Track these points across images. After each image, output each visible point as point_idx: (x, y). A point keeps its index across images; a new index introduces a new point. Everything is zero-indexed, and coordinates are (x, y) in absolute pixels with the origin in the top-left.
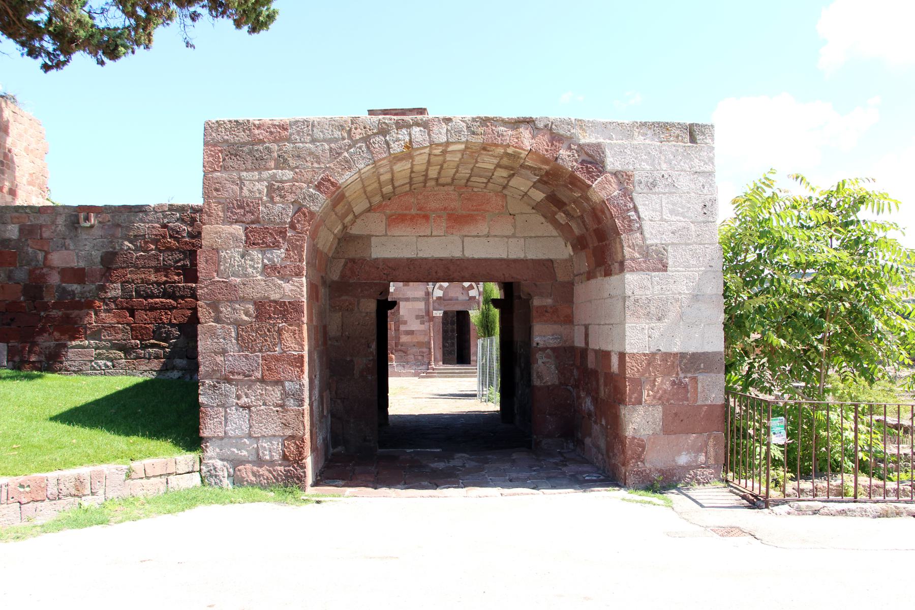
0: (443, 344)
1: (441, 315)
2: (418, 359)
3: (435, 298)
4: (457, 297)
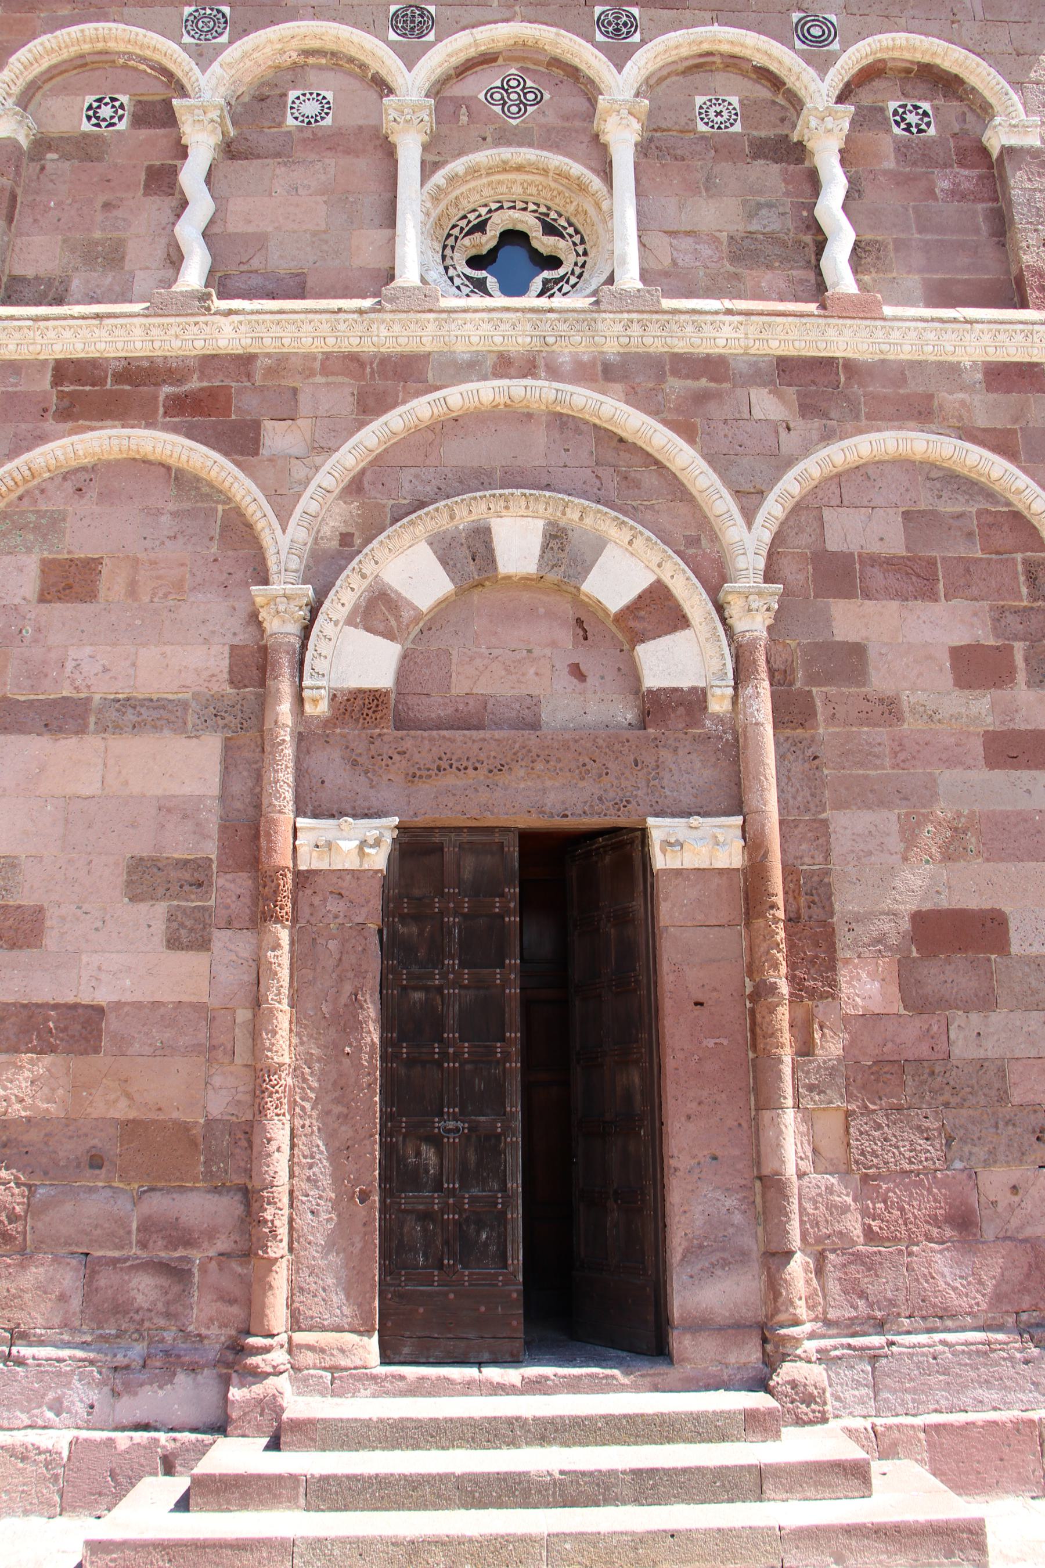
0: (389, 1151)
1: (378, 859)
2: (120, 1308)
3: (319, 708)
4: (534, 702)
